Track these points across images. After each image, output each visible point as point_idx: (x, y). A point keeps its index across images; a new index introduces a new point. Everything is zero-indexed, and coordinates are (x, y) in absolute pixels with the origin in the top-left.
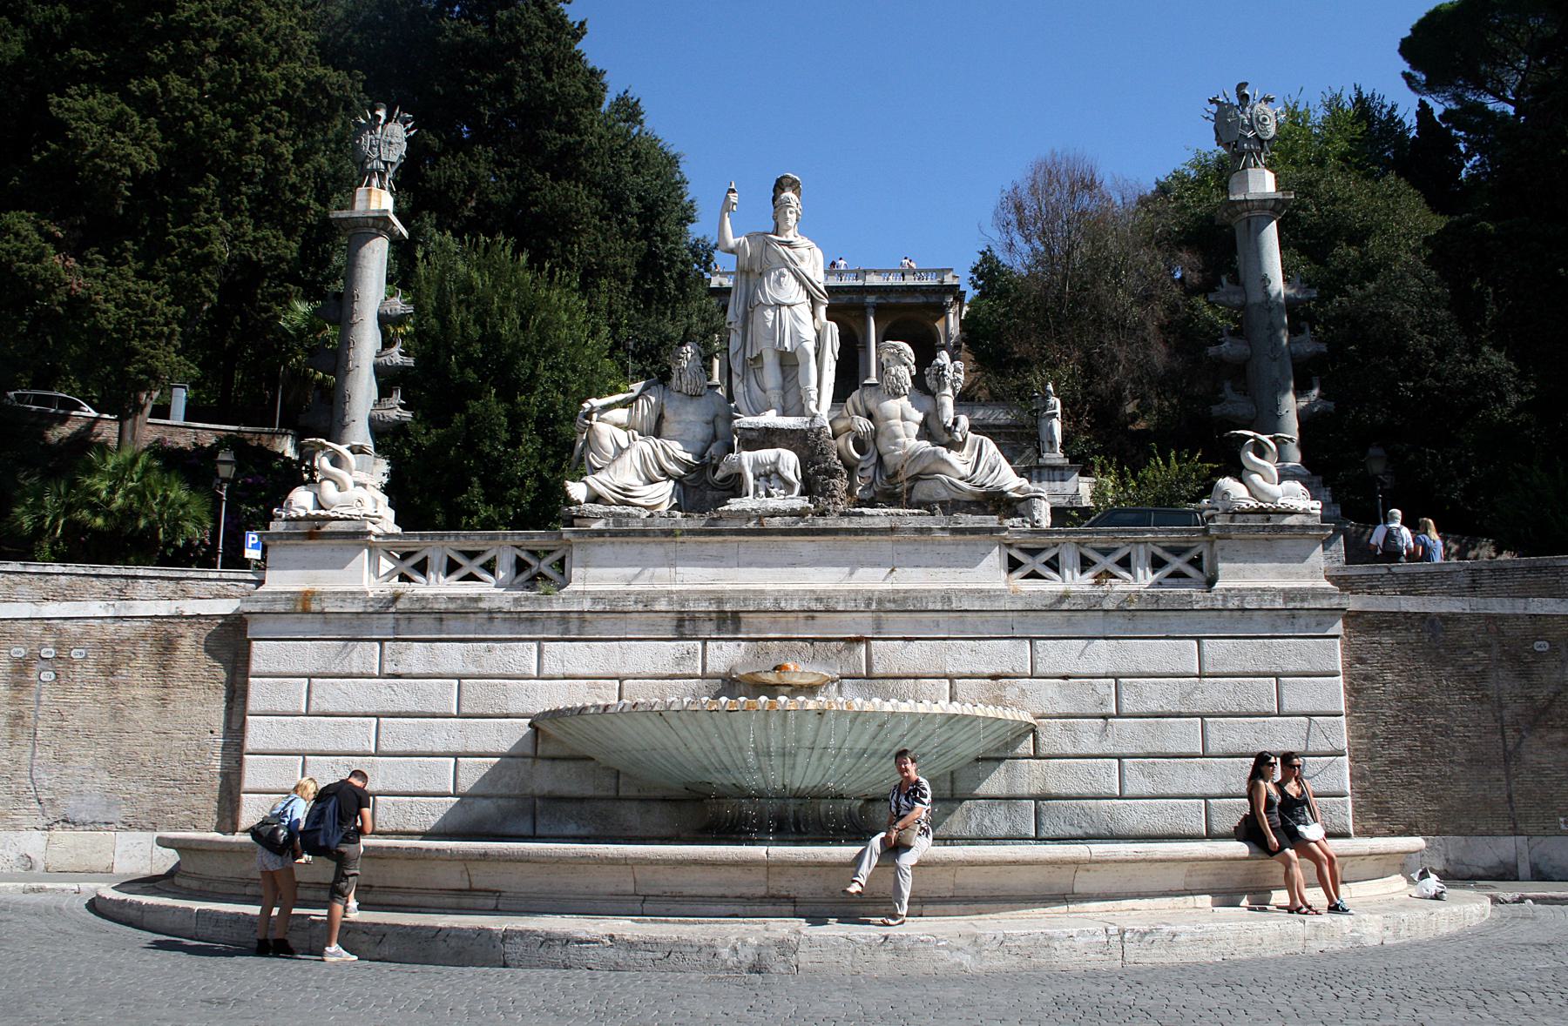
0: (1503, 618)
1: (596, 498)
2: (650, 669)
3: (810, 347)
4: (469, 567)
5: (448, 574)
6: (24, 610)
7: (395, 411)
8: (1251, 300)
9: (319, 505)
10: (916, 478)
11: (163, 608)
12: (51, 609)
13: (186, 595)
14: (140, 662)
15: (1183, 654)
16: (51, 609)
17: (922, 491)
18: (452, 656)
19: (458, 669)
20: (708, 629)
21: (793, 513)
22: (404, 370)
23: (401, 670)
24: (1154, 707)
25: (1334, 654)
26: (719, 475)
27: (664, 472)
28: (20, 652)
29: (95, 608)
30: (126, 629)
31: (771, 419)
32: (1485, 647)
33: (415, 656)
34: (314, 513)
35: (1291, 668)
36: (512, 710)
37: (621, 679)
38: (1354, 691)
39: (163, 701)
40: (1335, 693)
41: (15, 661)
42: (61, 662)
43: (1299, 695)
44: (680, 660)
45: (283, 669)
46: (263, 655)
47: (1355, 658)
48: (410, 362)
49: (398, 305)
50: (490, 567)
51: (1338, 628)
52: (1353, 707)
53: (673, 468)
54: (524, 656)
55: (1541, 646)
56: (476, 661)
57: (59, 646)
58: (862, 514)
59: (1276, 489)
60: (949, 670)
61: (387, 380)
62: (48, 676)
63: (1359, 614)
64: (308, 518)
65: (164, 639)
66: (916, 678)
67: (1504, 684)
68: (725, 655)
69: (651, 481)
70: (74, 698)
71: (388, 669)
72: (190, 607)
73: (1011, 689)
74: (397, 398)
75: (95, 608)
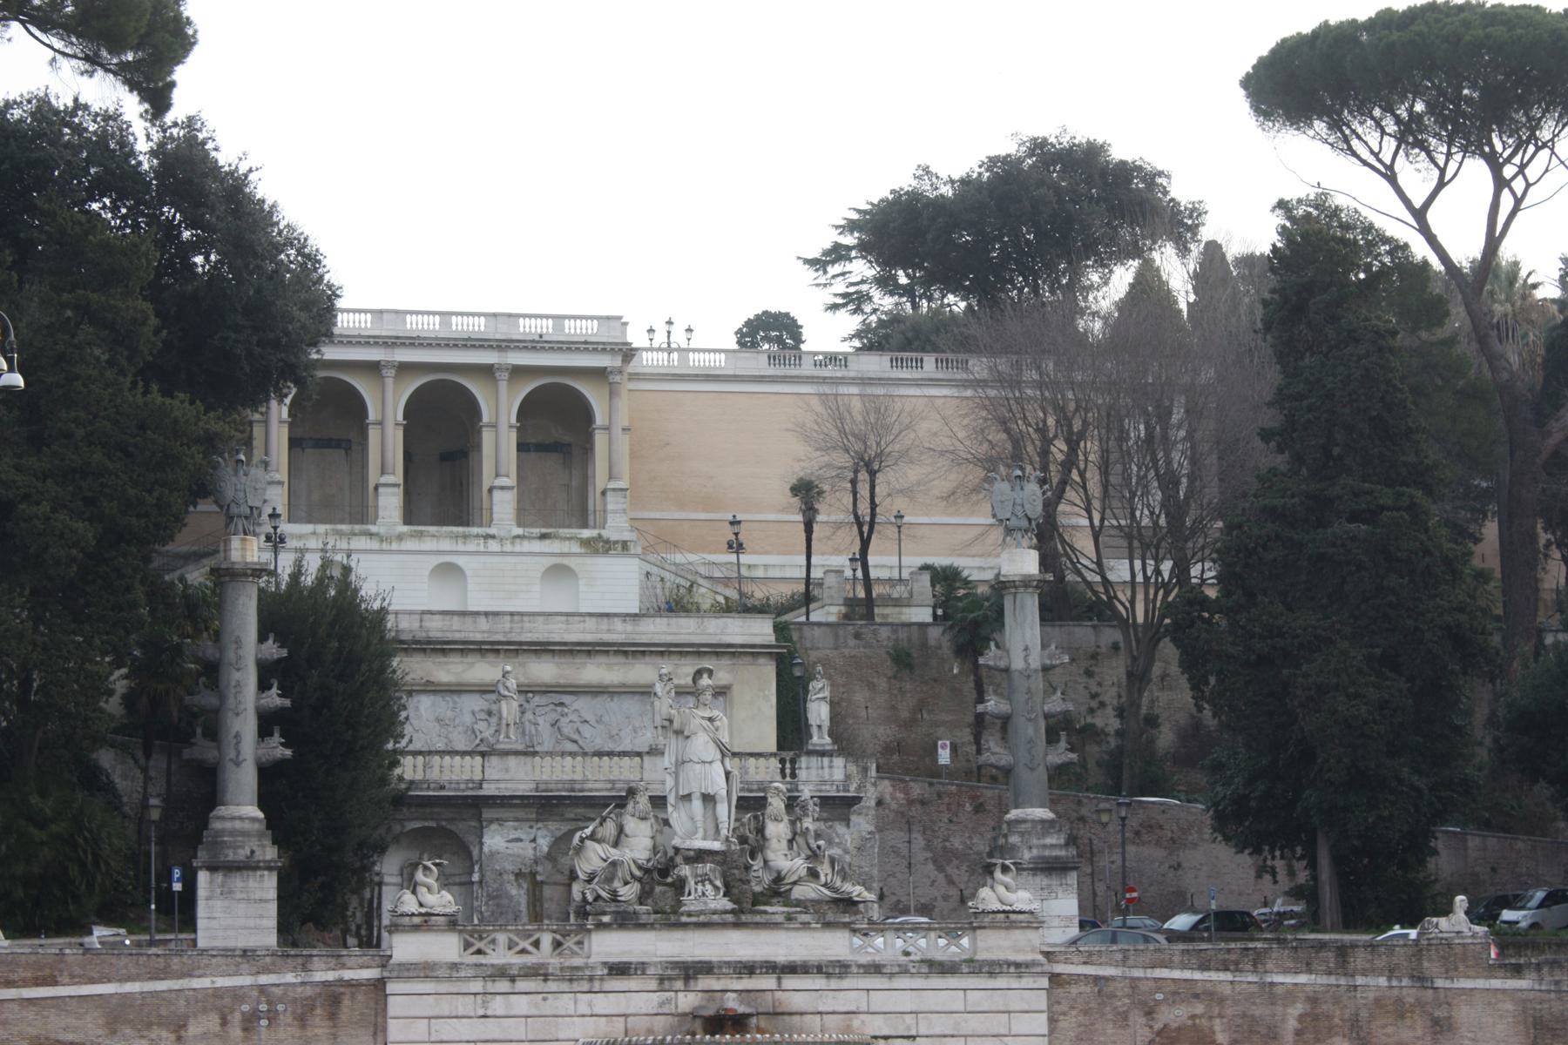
0: (1139, 979)
1: (598, 898)
2: (644, 1011)
3: (724, 792)
4: (526, 944)
5: (510, 948)
6: (246, 980)
7: (277, 749)
9: (421, 905)
10: (795, 883)
11: (331, 976)
12: (264, 979)
13: (344, 967)
14: (318, 1011)
15: (956, 1001)
16: (264, 979)
17: (798, 892)
18: (521, 1004)
19: (525, 1012)
20: (679, 984)
21: (726, 912)
22: (283, 709)
23: (489, 1013)
24: (937, 1031)
25: (1041, 1000)
26: (669, 880)
27: (633, 876)
28: (246, 1008)
29: (290, 978)
30: (309, 991)
31: (700, 843)
32: (1128, 996)
33: (498, 1005)
34: (423, 910)
35: (1017, 1008)
36: (561, 1036)
37: (626, 1016)
38: (1052, 1021)
39: (335, 1036)
40: (1040, 1023)
41: (243, 1013)
42: (272, 1016)
43: (1022, 1024)
44: (661, 1004)
45: (412, 1013)
46: (395, 1006)
47: (1053, 1002)
48: (287, 702)
49: (272, 650)
50: (536, 944)
51: (1044, 982)
52: (1052, 1031)
53: (638, 873)
54: (565, 1003)
55: (1159, 996)
56: (536, 1005)
57: (269, 1003)
58: (765, 912)
59: (1011, 897)
60: (820, 1009)
61: (267, 722)
62: (264, 1022)
63: (1059, 975)
64: (421, 914)
65: (332, 996)
66: (802, 1014)
67: (1137, 1019)
68: (687, 1001)
69: (626, 883)
70: (281, 1035)
71: (481, 1012)
72: (348, 975)
73: (856, 1022)
74: (277, 738)
75: (290, 978)
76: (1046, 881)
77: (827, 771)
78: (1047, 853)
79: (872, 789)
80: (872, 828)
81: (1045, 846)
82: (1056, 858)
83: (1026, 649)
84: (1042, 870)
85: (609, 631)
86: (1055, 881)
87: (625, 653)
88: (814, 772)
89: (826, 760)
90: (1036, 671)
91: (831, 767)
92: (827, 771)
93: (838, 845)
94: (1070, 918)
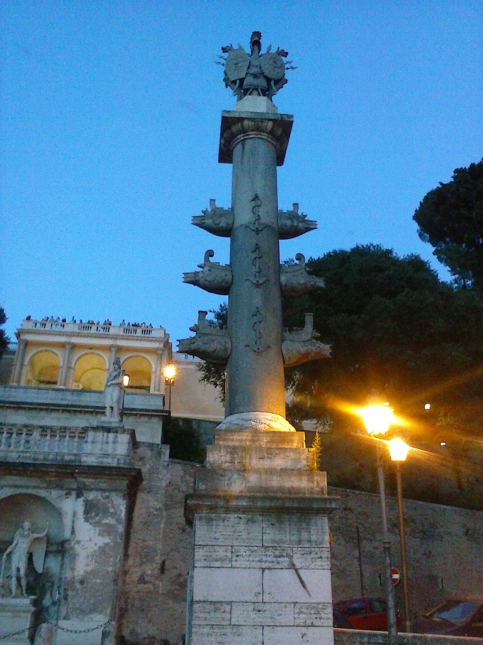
8: (238, 223)
76: (271, 534)
77: (111, 446)
78: (275, 482)
79: (164, 471)
80: (159, 505)
81: (271, 471)
82: (291, 490)
83: (256, 198)
84: (265, 512)
85: (62, 399)
86: (287, 535)
87: (69, 411)
88: (98, 446)
89: (111, 436)
90: (267, 226)
91: (115, 442)
92: (111, 446)
93: (113, 515)
94: (316, 609)
